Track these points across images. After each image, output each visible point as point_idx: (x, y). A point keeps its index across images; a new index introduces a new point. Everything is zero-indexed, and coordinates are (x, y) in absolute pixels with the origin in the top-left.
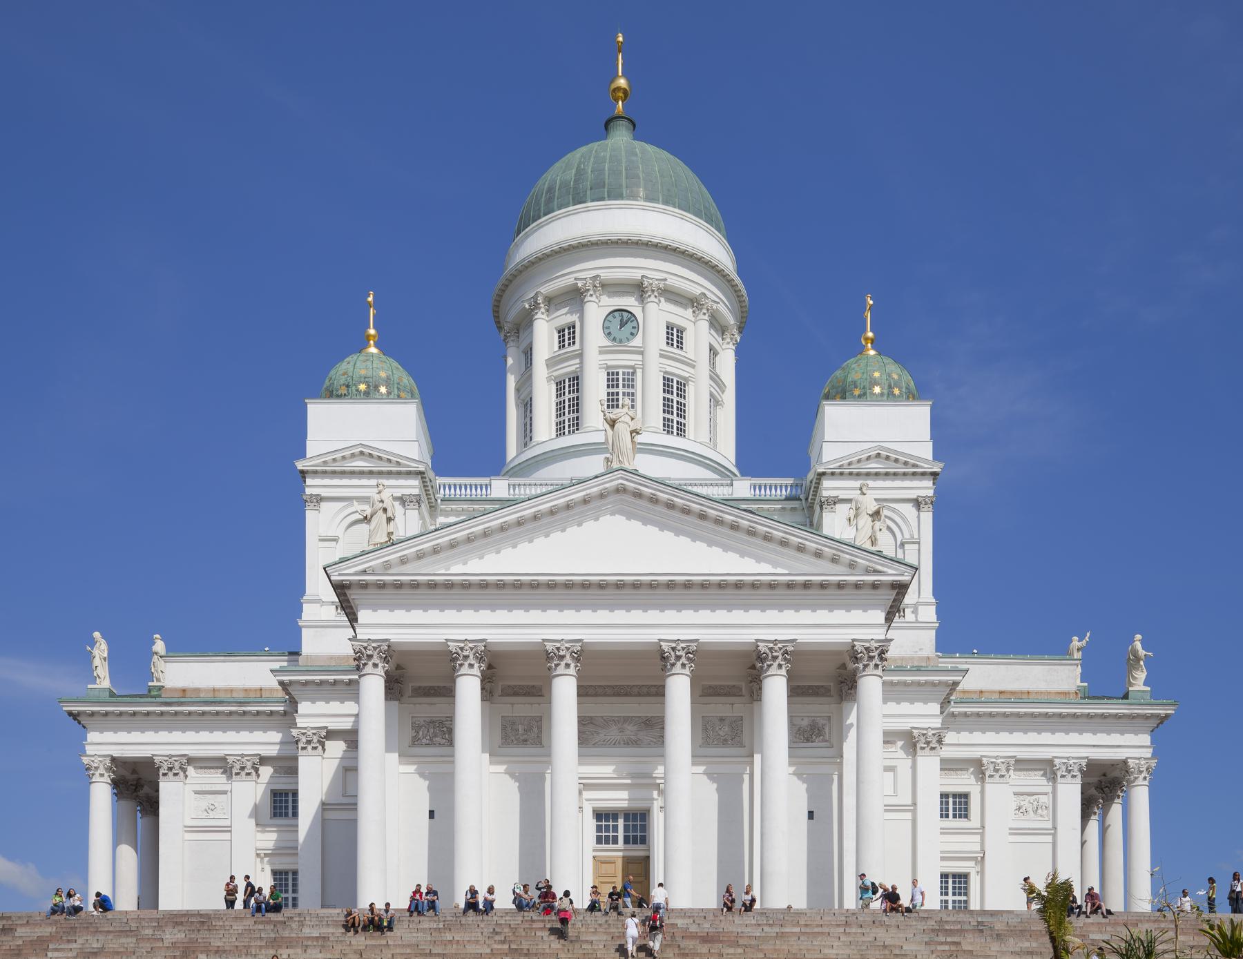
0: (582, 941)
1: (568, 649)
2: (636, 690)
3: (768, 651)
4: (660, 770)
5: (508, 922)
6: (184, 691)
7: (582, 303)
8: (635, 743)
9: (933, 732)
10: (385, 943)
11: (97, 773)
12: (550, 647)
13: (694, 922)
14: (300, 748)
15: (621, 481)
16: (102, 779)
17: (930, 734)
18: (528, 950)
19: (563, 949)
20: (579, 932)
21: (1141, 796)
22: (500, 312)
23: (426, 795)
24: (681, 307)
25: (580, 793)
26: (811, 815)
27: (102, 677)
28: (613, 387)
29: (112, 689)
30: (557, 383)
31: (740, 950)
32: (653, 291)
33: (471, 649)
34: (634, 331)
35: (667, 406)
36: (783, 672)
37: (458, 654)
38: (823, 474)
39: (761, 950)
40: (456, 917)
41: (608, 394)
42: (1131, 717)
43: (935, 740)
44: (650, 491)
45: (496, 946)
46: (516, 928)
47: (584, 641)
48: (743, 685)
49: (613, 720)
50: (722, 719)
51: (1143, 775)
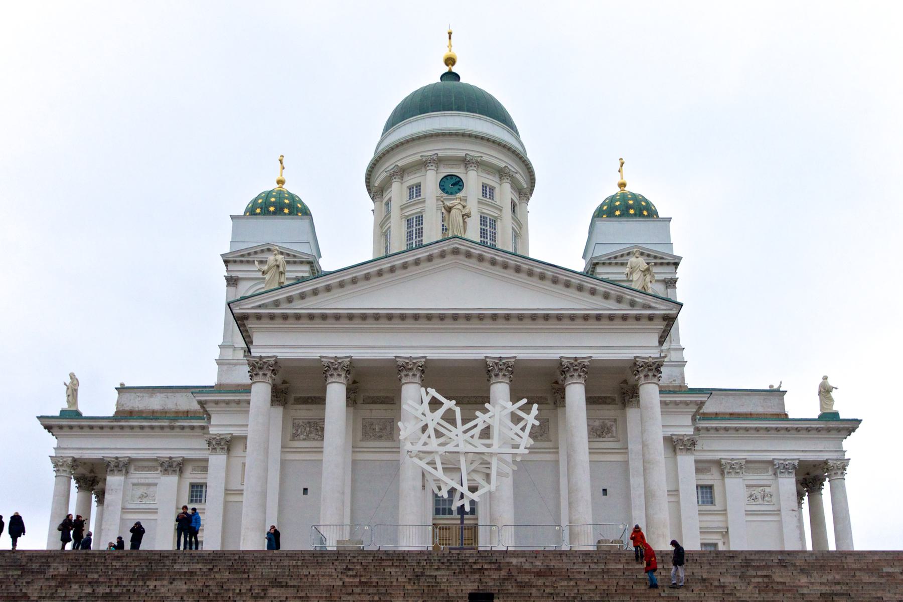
0: (427, 576)
1: (415, 363)
5: (359, 561)
12: (400, 362)
13: (527, 560)
17: (685, 439)
18: (377, 583)
19: (409, 583)
20: (424, 569)
22: (371, 180)
30: (408, 220)
31: (572, 583)
34: (462, 184)
37: (329, 367)
38: (597, 264)
39: (592, 583)
40: (314, 557)
45: (347, 580)
46: (367, 566)
47: (427, 358)
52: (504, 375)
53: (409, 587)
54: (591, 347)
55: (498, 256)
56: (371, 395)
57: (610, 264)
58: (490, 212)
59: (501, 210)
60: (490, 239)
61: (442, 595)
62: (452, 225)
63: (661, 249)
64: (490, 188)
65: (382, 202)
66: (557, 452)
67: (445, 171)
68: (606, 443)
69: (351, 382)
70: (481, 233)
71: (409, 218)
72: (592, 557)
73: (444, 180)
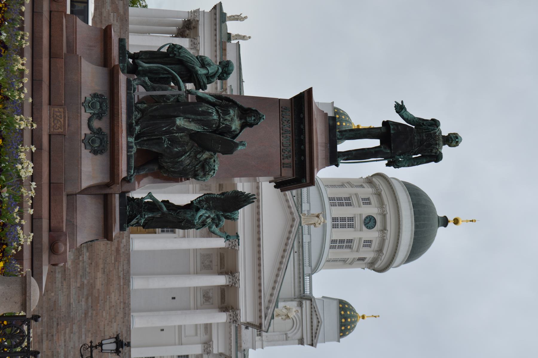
28: (348, 220)
31: (113, 262)
35: (342, 241)
41: (345, 218)
52: (230, 244)
54: (245, 287)
55: (291, 241)
57: (312, 308)
58: (355, 245)
59: (357, 251)
60: (339, 245)
62: (310, 218)
63: (321, 336)
64: (370, 245)
65: (364, 183)
66: (194, 274)
67: (378, 219)
68: (200, 299)
70: (342, 240)
71: (350, 199)
73: (373, 218)
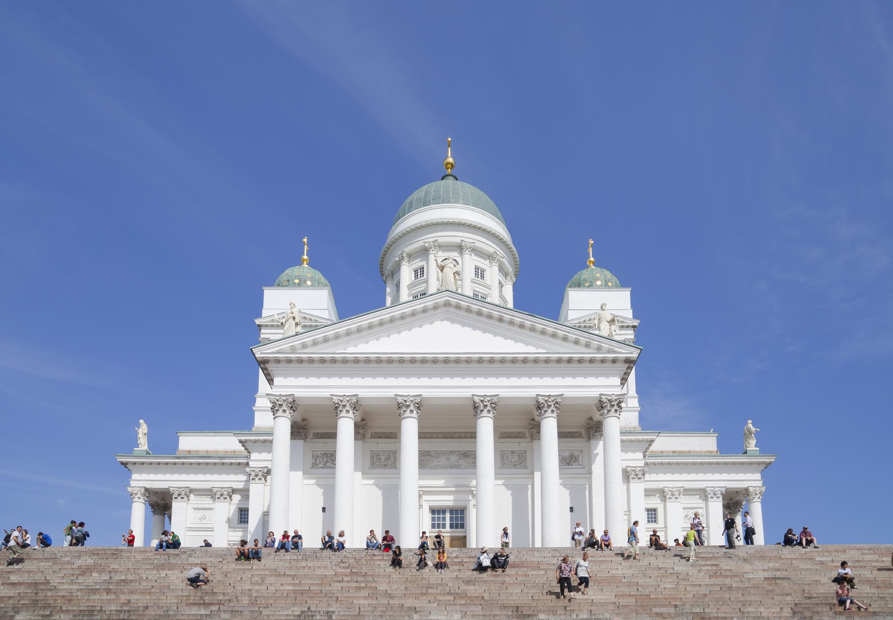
1: (412, 401)
2: (457, 435)
3: (545, 402)
4: (474, 483)
6: (189, 452)
7: (428, 254)
8: (457, 467)
9: (640, 469)
10: (251, 568)
11: (136, 497)
12: (400, 400)
14: (251, 479)
15: (447, 298)
16: (139, 500)
18: (366, 573)
21: (756, 509)
23: (322, 498)
24: (483, 259)
25: (420, 496)
26: (571, 509)
27: (143, 444)
29: (148, 451)
31: (542, 572)
32: (467, 248)
33: (348, 401)
36: (555, 415)
42: (751, 464)
43: (640, 473)
44: (466, 304)
46: (359, 560)
48: (526, 431)
49: (443, 453)
50: (513, 452)
51: (758, 496)
53: (395, 576)
56: (377, 431)
61: (423, 582)
69: (359, 420)
72: (560, 552)
